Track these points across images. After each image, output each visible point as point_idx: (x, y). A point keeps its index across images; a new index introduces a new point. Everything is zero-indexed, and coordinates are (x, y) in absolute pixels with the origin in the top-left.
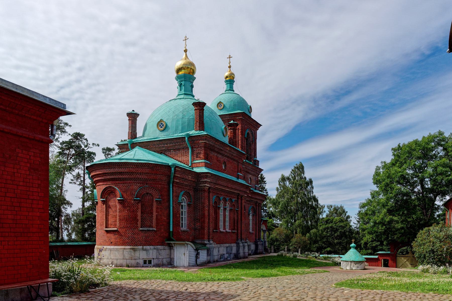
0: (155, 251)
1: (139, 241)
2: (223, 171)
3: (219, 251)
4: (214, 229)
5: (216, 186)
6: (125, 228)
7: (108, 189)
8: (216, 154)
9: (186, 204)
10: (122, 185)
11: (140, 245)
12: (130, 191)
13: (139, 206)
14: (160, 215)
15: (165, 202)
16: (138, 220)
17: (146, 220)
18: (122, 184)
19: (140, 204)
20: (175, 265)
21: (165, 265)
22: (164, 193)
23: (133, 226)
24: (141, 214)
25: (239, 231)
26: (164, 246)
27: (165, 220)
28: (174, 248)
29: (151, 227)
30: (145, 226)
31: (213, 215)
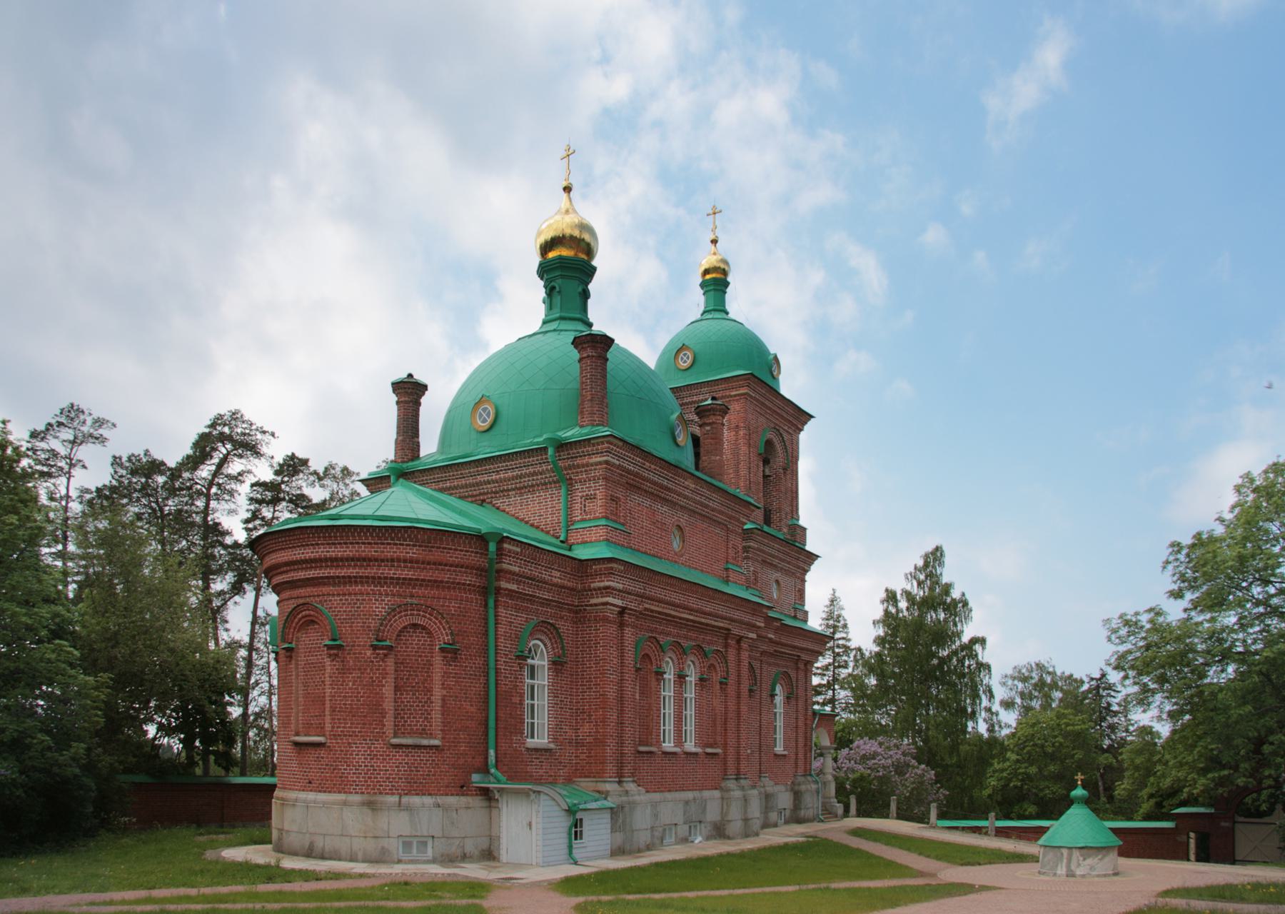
0: (439, 812)
1: (387, 778)
2: (674, 559)
3: (656, 816)
4: (640, 745)
5: (647, 606)
6: (346, 735)
7: (302, 611)
8: (647, 503)
9: (546, 663)
10: (341, 600)
11: (393, 794)
12: (361, 619)
13: (386, 666)
14: (457, 697)
15: (470, 655)
16: (383, 714)
17: (411, 714)
18: (339, 595)
19: (390, 662)
20: (504, 857)
21: (471, 857)
22: (470, 625)
23: (371, 732)
24: (396, 695)
25: (731, 751)
26: (469, 799)
27: (472, 713)
28: (500, 806)
29: (427, 734)
30: (408, 733)
31: (638, 698)
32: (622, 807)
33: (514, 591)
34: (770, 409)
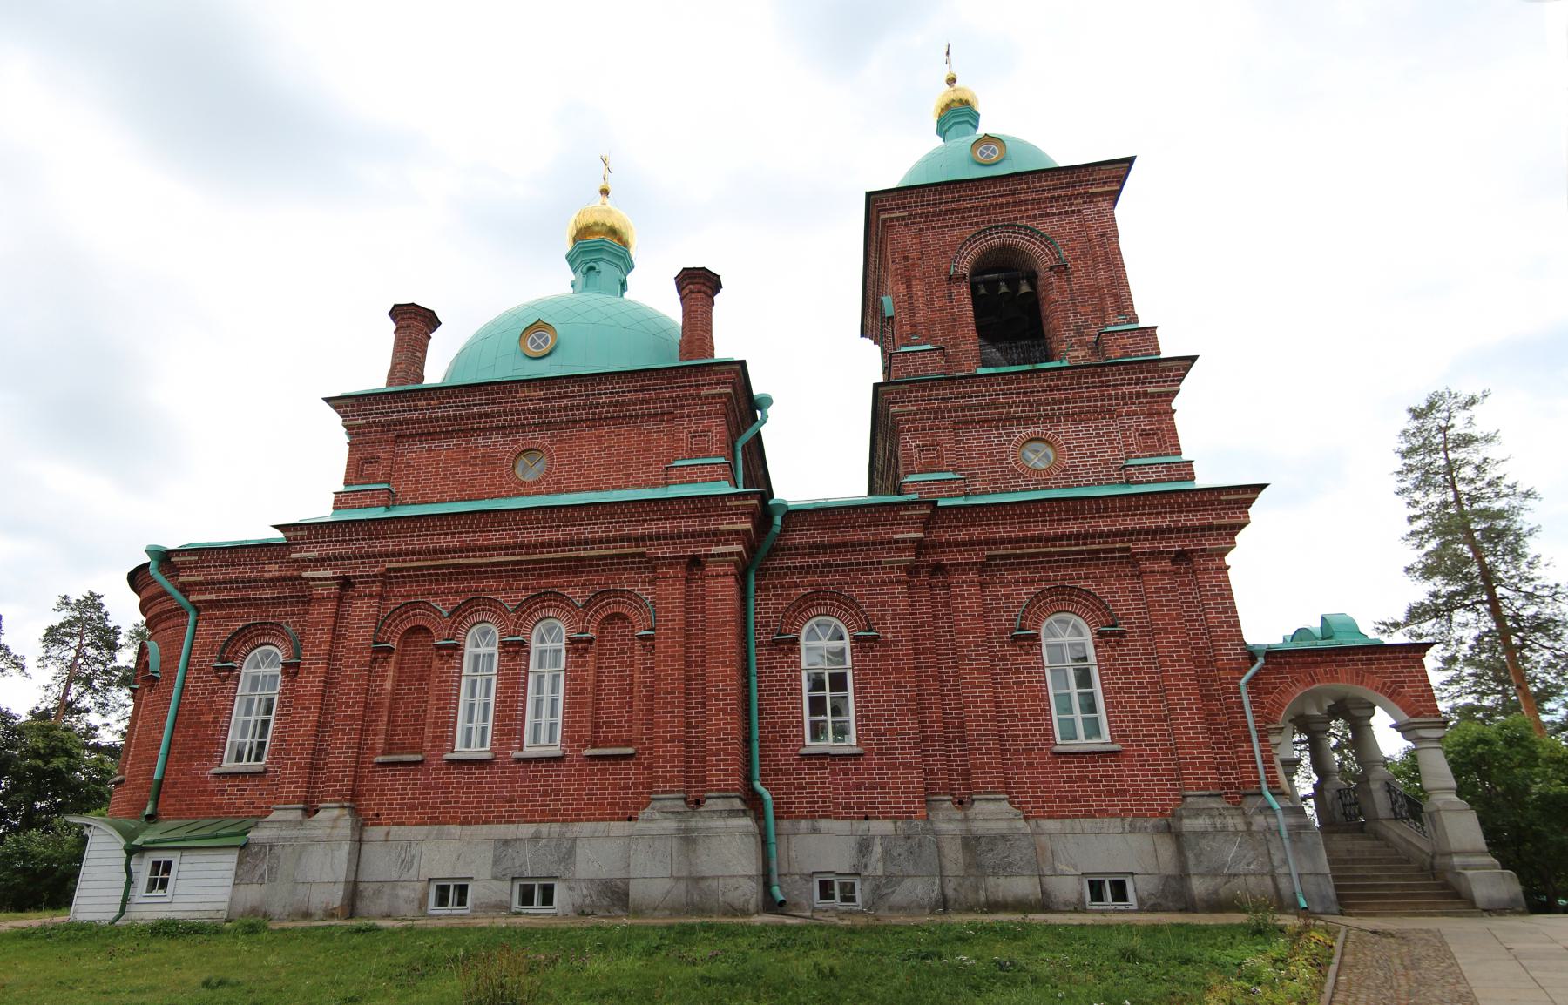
5: (387, 565)
32: (272, 847)
33: (212, 601)
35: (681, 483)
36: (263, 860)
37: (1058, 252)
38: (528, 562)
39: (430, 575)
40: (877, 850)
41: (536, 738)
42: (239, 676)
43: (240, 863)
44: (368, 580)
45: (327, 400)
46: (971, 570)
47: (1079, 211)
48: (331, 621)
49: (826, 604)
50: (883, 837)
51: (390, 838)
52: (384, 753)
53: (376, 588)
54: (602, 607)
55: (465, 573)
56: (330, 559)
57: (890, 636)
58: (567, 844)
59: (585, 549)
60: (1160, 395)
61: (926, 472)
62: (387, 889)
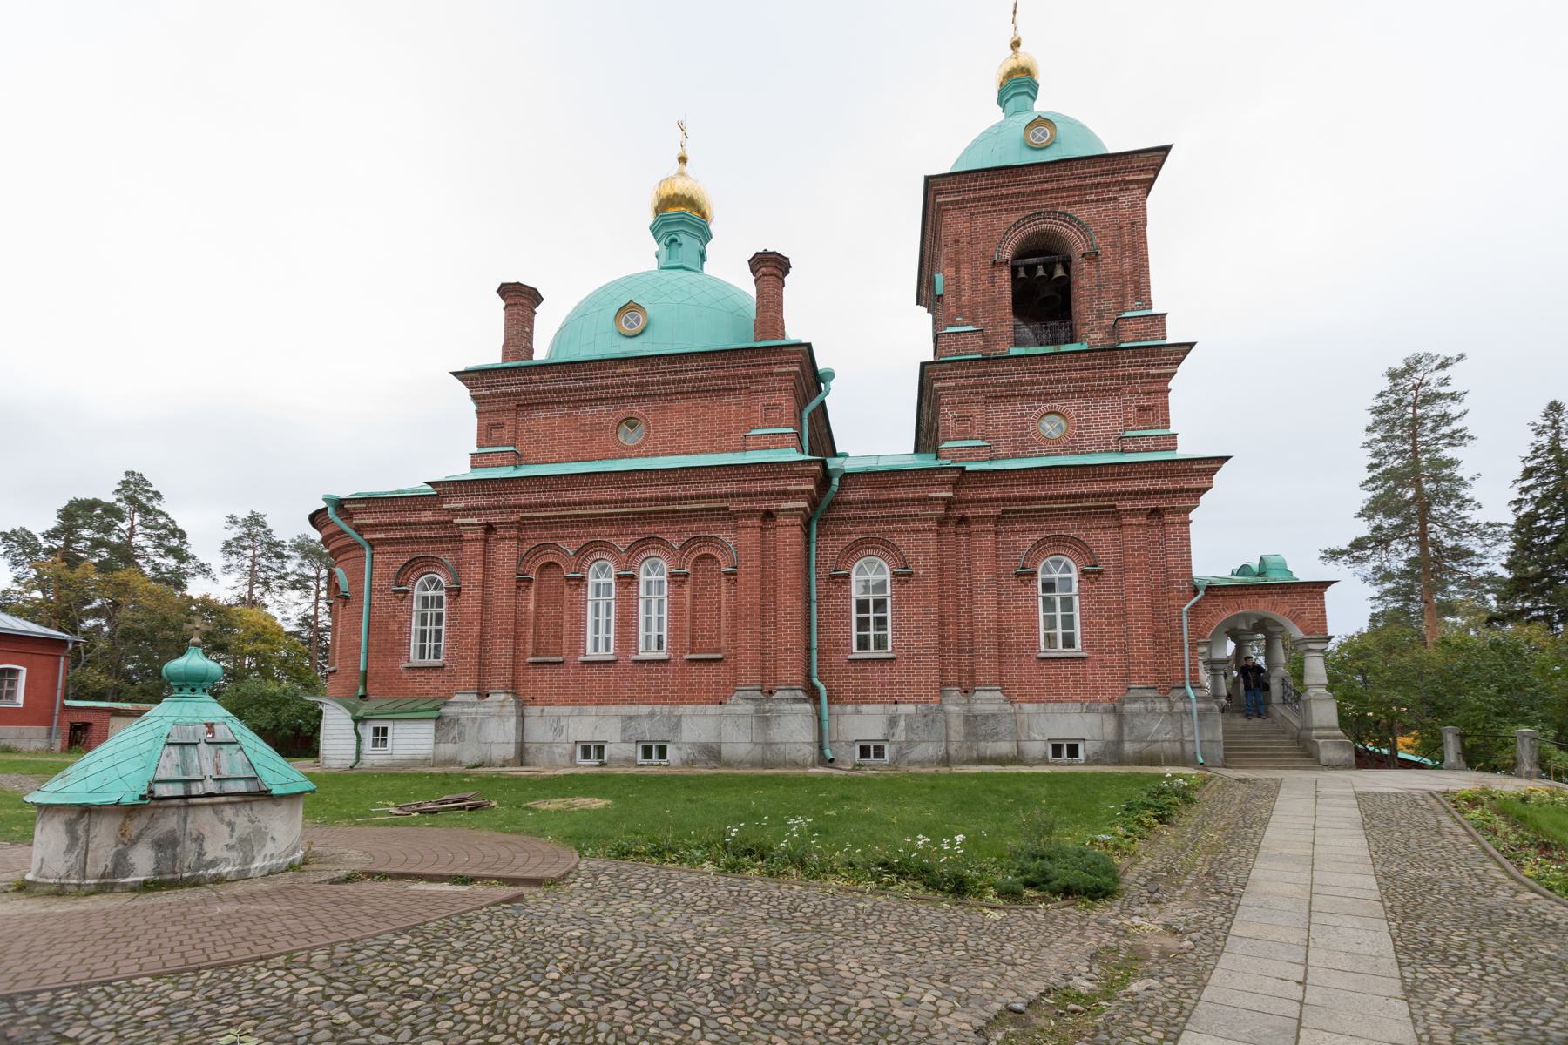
32: (458, 719)
34: (1017, 195)
35: (757, 449)
36: (453, 727)
37: (1091, 240)
38: (634, 513)
39: (556, 523)
40: (902, 724)
41: (648, 646)
42: (412, 597)
43: (437, 729)
44: (507, 526)
45: (455, 374)
46: (989, 521)
47: (1115, 198)
48: (481, 558)
49: (873, 548)
50: (907, 715)
51: (545, 714)
52: (533, 656)
53: (514, 532)
54: (695, 549)
55: (584, 521)
56: (474, 509)
57: (921, 572)
58: (675, 720)
59: (680, 504)
60: (1159, 376)
61: (960, 439)
62: (546, 748)
